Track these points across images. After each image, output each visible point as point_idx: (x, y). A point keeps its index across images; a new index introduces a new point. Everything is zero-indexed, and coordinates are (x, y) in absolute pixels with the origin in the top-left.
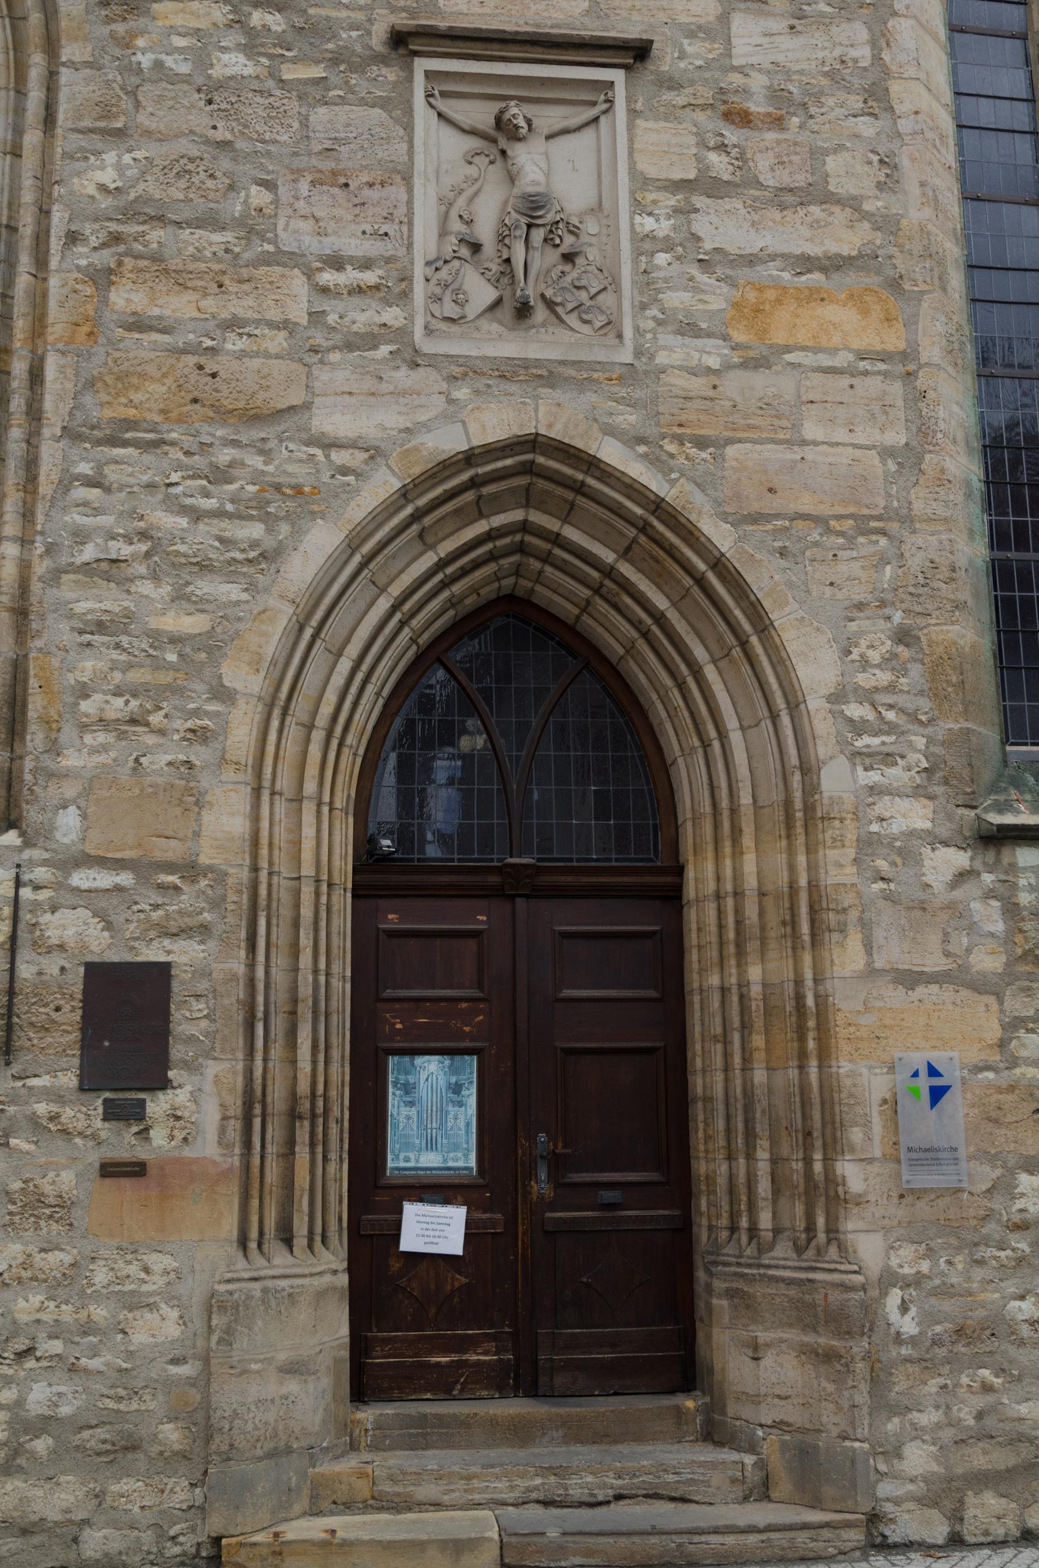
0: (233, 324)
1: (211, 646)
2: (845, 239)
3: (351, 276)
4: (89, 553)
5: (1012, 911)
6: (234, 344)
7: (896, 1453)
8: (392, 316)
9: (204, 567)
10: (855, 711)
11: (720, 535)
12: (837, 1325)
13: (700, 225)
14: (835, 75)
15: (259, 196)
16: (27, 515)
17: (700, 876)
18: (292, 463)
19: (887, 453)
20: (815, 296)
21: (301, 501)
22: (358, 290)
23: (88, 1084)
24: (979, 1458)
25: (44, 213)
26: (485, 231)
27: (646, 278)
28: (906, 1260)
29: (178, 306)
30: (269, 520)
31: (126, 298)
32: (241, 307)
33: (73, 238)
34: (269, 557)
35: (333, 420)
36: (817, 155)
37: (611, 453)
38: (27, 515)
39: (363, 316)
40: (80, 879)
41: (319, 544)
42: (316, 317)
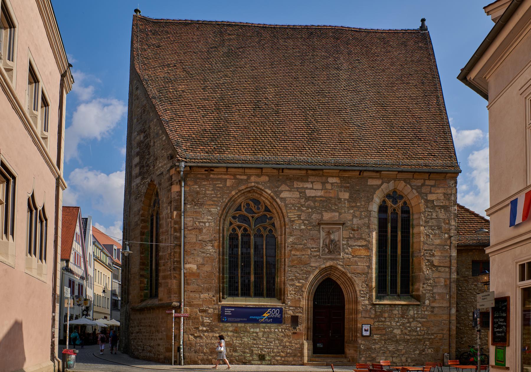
0: (303, 255)
1: (301, 287)
2: (364, 243)
3: (314, 249)
4: (290, 278)
5: (375, 311)
6: (303, 257)
7: (361, 358)
8: (318, 253)
9: (301, 279)
10: (362, 292)
11: (349, 275)
12: (357, 349)
13: (349, 242)
14: (364, 224)
15: (305, 241)
16: (284, 274)
17: (346, 307)
18: (309, 269)
19: (367, 266)
20: (360, 250)
21: (309, 273)
22: (315, 251)
23: (291, 326)
24: (368, 359)
25: (285, 243)
26: (327, 243)
27: (344, 249)
28: (363, 342)
29: (298, 253)
30: (307, 275)
31: (293, 252)
32: (304, 253)
33: (288, 247)
34: (307, 278)
35: (313, 264)
36: (362, 234)
37: (339, 267)
38: (284, 274)
39: (315, 254)
40: (291, 308)
41: (312, 277)
42: (311, 254)
